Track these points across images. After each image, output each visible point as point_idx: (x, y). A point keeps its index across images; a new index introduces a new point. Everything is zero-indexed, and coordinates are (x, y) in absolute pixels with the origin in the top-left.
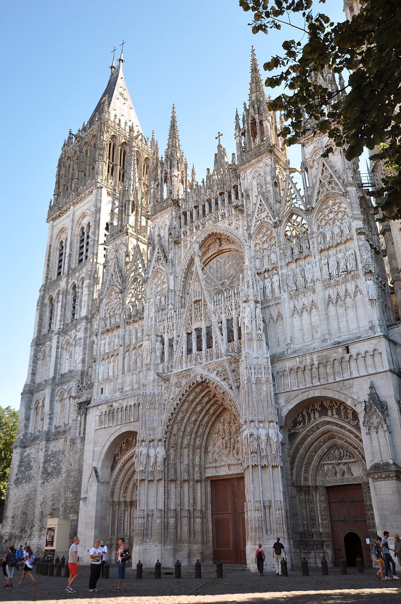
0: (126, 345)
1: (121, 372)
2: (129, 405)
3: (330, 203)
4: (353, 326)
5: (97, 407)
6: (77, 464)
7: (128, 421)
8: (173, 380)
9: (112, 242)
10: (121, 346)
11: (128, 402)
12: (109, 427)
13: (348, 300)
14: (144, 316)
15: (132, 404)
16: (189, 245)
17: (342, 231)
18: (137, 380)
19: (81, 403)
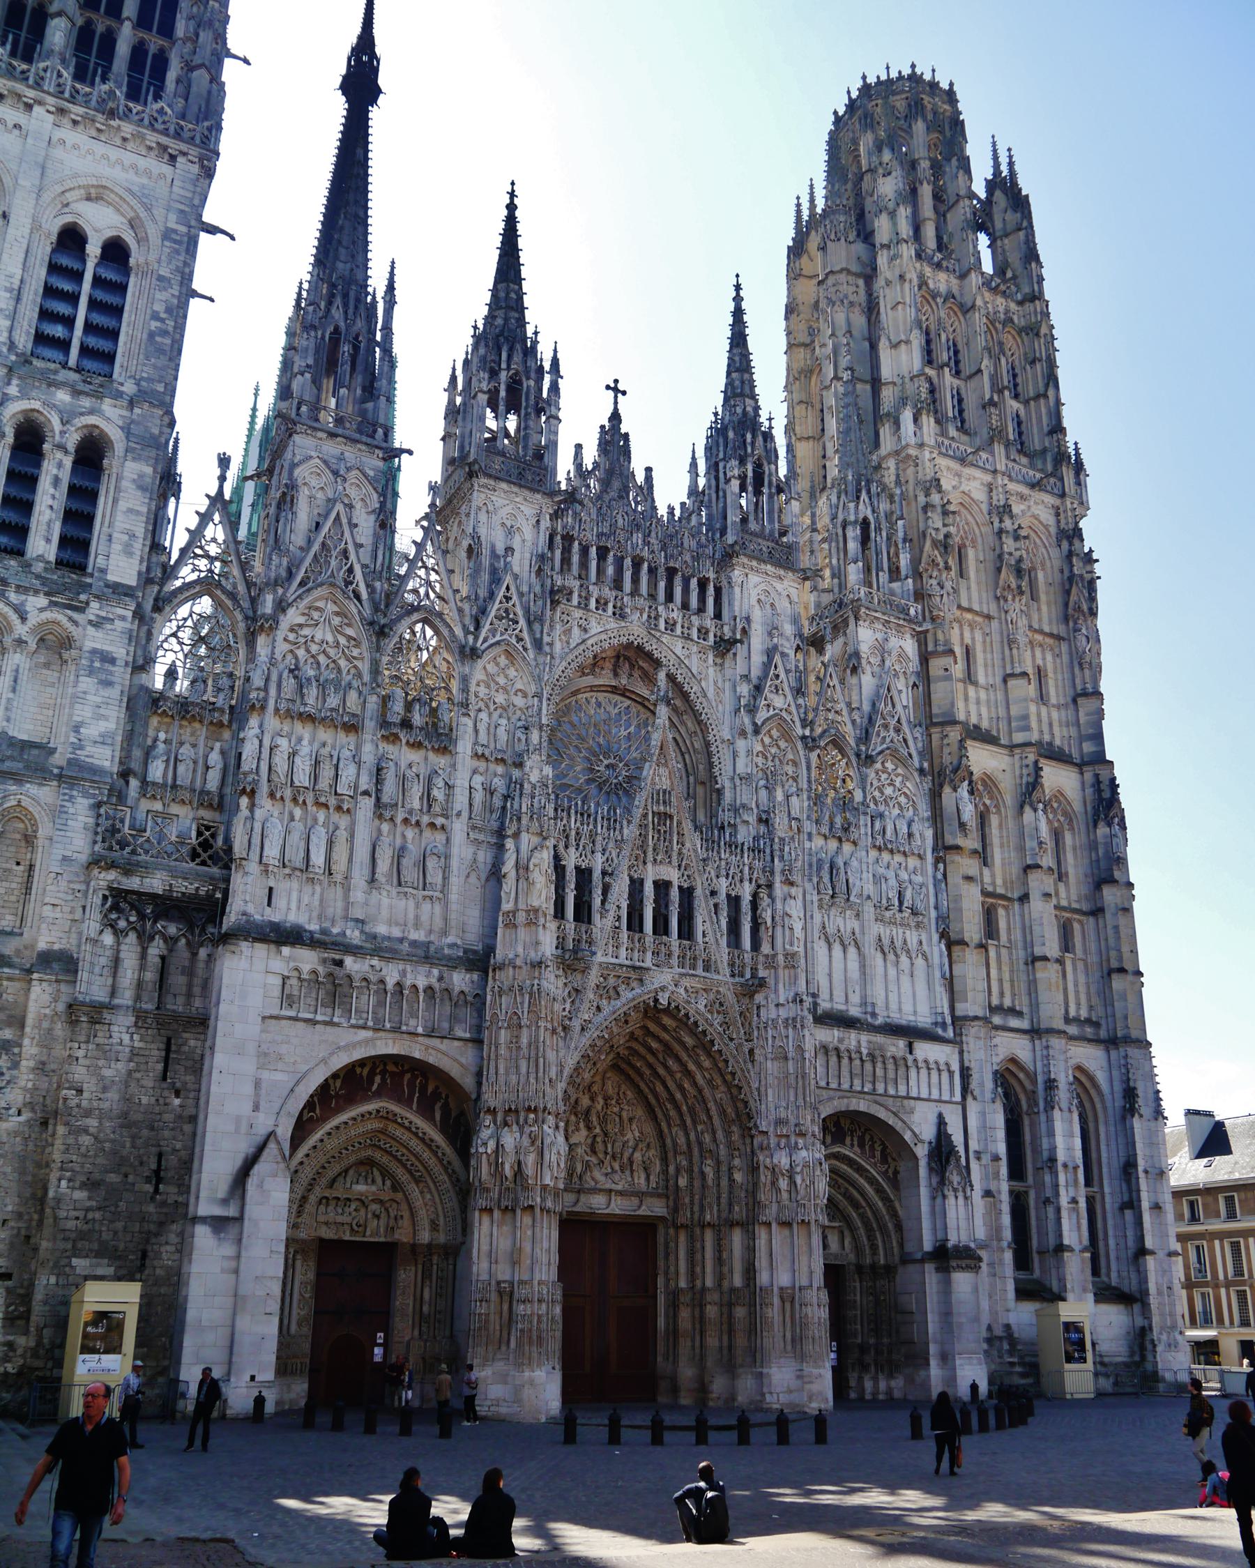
0: (385, 799)
1: (367, 872)
2: (408, 983)
3: (889, 766)
4: (907, 1008)
5: (272, 947)
6: (113, 1095)
7: (404, 1028)
8: (594, 977)
9: (320, 434)
10: (366, 793)
11: (403, 973)
12: (326, 1023)
13: (904, 959)
14: (460, 748)
15: (421, 986)
16: (576, 631)
17: (910, 835)
18: (417, 917)
19: (128, 892)
